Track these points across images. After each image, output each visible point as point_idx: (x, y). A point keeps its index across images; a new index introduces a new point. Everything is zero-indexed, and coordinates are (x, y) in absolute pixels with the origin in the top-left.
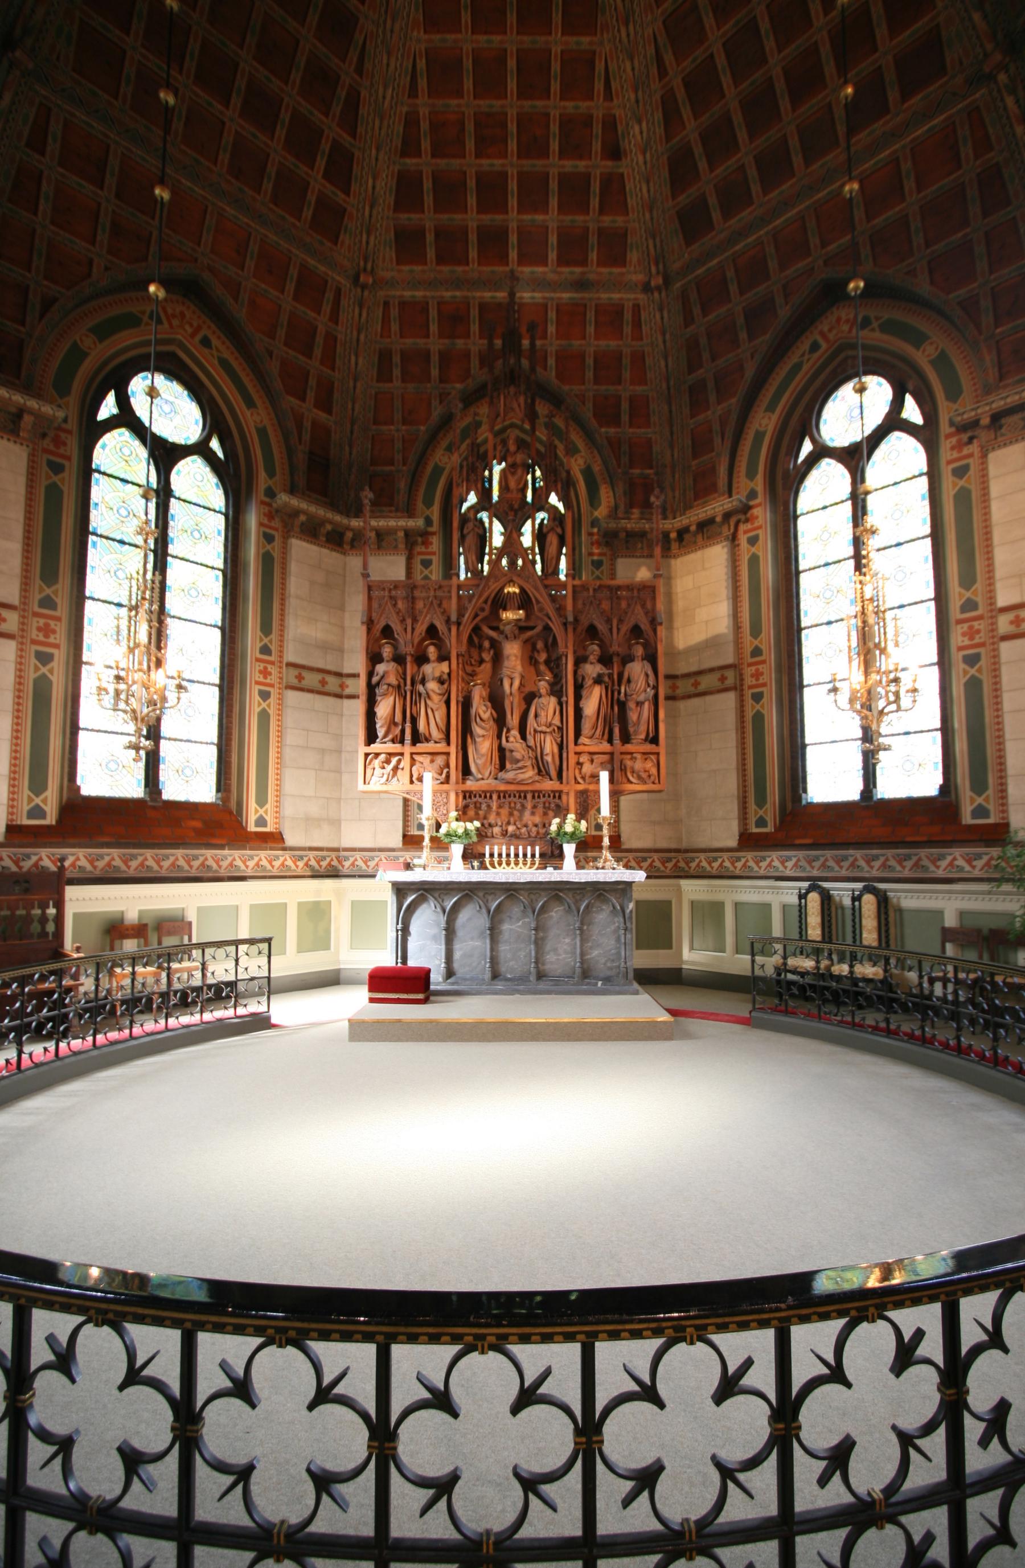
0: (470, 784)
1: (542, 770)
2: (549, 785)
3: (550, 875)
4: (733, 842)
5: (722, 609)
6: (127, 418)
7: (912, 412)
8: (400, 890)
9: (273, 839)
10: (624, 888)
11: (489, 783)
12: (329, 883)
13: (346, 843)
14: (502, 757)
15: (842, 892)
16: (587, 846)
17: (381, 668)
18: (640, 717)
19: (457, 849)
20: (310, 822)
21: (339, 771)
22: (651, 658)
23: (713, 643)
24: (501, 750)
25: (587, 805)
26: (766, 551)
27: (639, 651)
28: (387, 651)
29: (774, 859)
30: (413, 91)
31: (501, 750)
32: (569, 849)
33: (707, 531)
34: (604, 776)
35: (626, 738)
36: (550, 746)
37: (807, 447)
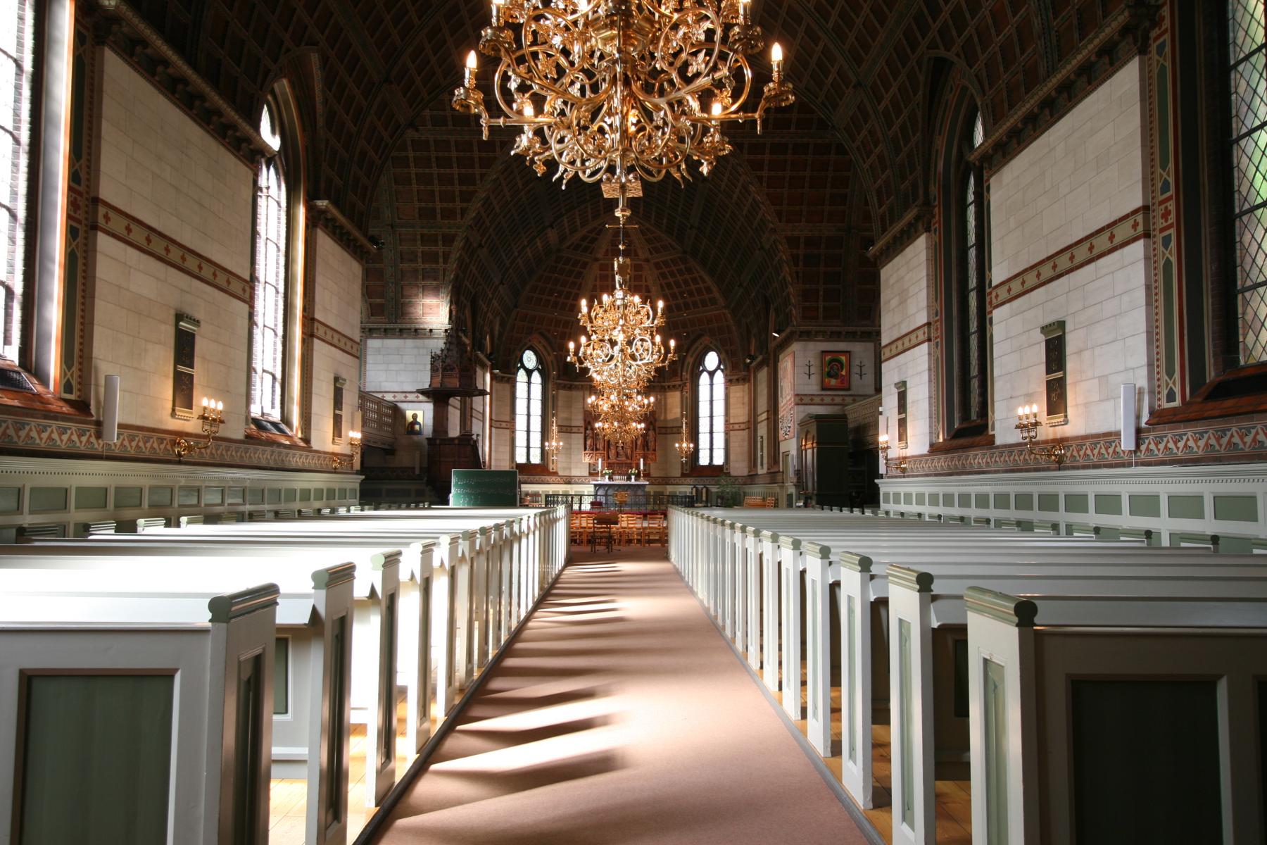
0: (610, 461)
1: (627, 457)
2: (629, 461)
3: (628, 482)
4: (679, 475)
5: (678, 410)
6: (523, 366)
7: (722, 367)
8: (595, 485)
9: (555, 474)
10: (644, 486)
11: (614, 461)
12: (569, 486)
13: (573, 475)
14: (618, 454)
15: (700, 487)
16: (638, 476)
17: (588, 432)
18: (651, 444)
19: (607, 477)
20: (564, 469)
21: (571, 454)
22: (654, 430)
23: (676, 419)
24: (617, 453)
25: (638, 467)
26: (688, 395)
27: (651, 428)
28: (589, 428)
29: (689, 480)
30: (596, 281)
31: (617, 453)
32: (633, 477)
33: (674, 388)
34: (642, 460)
35: (648, 450)
36: (629, 451)
37: (701, 368)
